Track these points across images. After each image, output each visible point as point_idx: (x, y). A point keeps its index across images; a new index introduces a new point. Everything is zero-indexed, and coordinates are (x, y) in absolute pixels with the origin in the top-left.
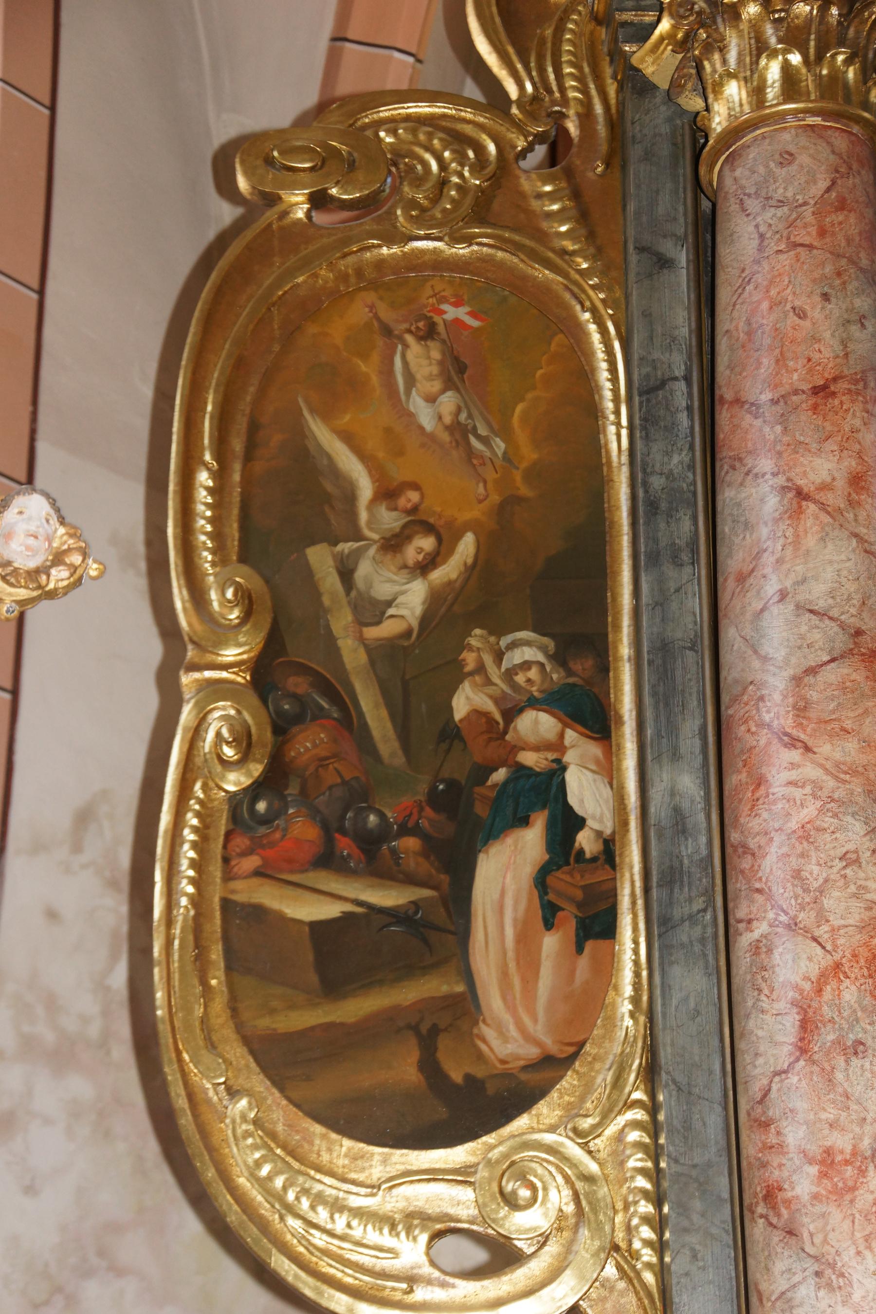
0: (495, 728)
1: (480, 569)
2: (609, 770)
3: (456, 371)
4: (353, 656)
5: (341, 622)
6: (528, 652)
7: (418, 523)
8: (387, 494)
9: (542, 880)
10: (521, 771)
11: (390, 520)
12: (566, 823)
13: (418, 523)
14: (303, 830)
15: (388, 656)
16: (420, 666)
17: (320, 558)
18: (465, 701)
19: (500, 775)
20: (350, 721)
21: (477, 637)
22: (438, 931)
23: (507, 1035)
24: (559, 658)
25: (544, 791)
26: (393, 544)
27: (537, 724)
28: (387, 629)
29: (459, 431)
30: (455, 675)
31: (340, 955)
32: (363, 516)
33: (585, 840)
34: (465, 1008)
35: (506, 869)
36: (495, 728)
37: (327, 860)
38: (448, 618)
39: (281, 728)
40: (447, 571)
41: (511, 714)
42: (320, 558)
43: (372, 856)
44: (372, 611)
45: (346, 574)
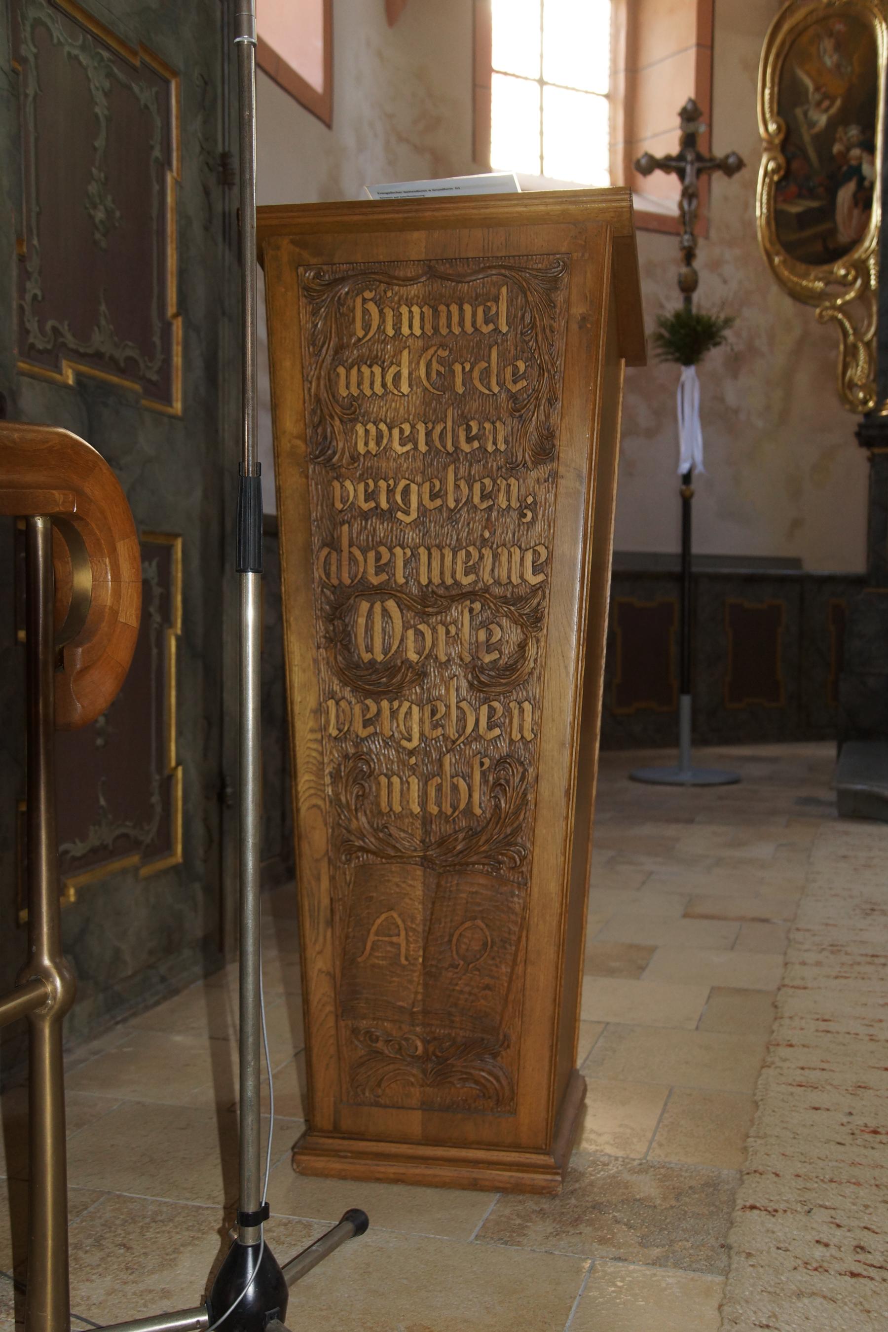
0: (844, 155)
1: (843, 110)
2: (873, 163)
3: (838, 47)
4: (807, 138)
5: (804, 129)
6: (854, 132)
7: (826, 96)
8: (817, 89)
9: (855, 195)
10: (851, 167)
11: (818, 97)
12: (862, 179)
13: (826, 96)
14: (793, 188)
15: (817, 138)
16: (825, 139)
17: (799, 111)
18: (837, 148)
19: (845, 168)
20: (806, 157)
21: (840, 130)
22: (828, 211)
23: (844, 236)
24: (863, 132)
25: (856, 173)
26: (819, 104)
27: (856, 152)
28: (816, 130)
29: (838, 66)
30: (833, 141)
31: (803, 220)
32: (810, 96)
33: (866, 183)
34: (833, 231)
35: (845, 194)
36: (844, 155)
37: (800, 196)
38: (832, 124)
39: (788, 162)
40: (833, 111)
41: (848, 149)
42: (799, 111)
43: (811, 194)
44: (812, 124)
45: (805, 114)
